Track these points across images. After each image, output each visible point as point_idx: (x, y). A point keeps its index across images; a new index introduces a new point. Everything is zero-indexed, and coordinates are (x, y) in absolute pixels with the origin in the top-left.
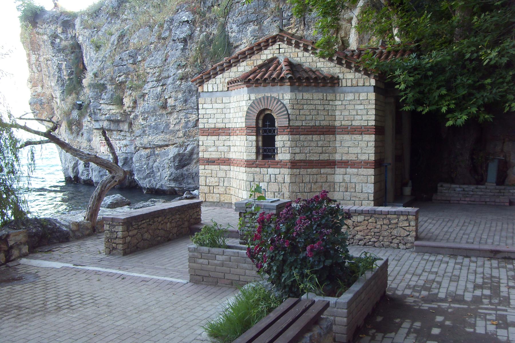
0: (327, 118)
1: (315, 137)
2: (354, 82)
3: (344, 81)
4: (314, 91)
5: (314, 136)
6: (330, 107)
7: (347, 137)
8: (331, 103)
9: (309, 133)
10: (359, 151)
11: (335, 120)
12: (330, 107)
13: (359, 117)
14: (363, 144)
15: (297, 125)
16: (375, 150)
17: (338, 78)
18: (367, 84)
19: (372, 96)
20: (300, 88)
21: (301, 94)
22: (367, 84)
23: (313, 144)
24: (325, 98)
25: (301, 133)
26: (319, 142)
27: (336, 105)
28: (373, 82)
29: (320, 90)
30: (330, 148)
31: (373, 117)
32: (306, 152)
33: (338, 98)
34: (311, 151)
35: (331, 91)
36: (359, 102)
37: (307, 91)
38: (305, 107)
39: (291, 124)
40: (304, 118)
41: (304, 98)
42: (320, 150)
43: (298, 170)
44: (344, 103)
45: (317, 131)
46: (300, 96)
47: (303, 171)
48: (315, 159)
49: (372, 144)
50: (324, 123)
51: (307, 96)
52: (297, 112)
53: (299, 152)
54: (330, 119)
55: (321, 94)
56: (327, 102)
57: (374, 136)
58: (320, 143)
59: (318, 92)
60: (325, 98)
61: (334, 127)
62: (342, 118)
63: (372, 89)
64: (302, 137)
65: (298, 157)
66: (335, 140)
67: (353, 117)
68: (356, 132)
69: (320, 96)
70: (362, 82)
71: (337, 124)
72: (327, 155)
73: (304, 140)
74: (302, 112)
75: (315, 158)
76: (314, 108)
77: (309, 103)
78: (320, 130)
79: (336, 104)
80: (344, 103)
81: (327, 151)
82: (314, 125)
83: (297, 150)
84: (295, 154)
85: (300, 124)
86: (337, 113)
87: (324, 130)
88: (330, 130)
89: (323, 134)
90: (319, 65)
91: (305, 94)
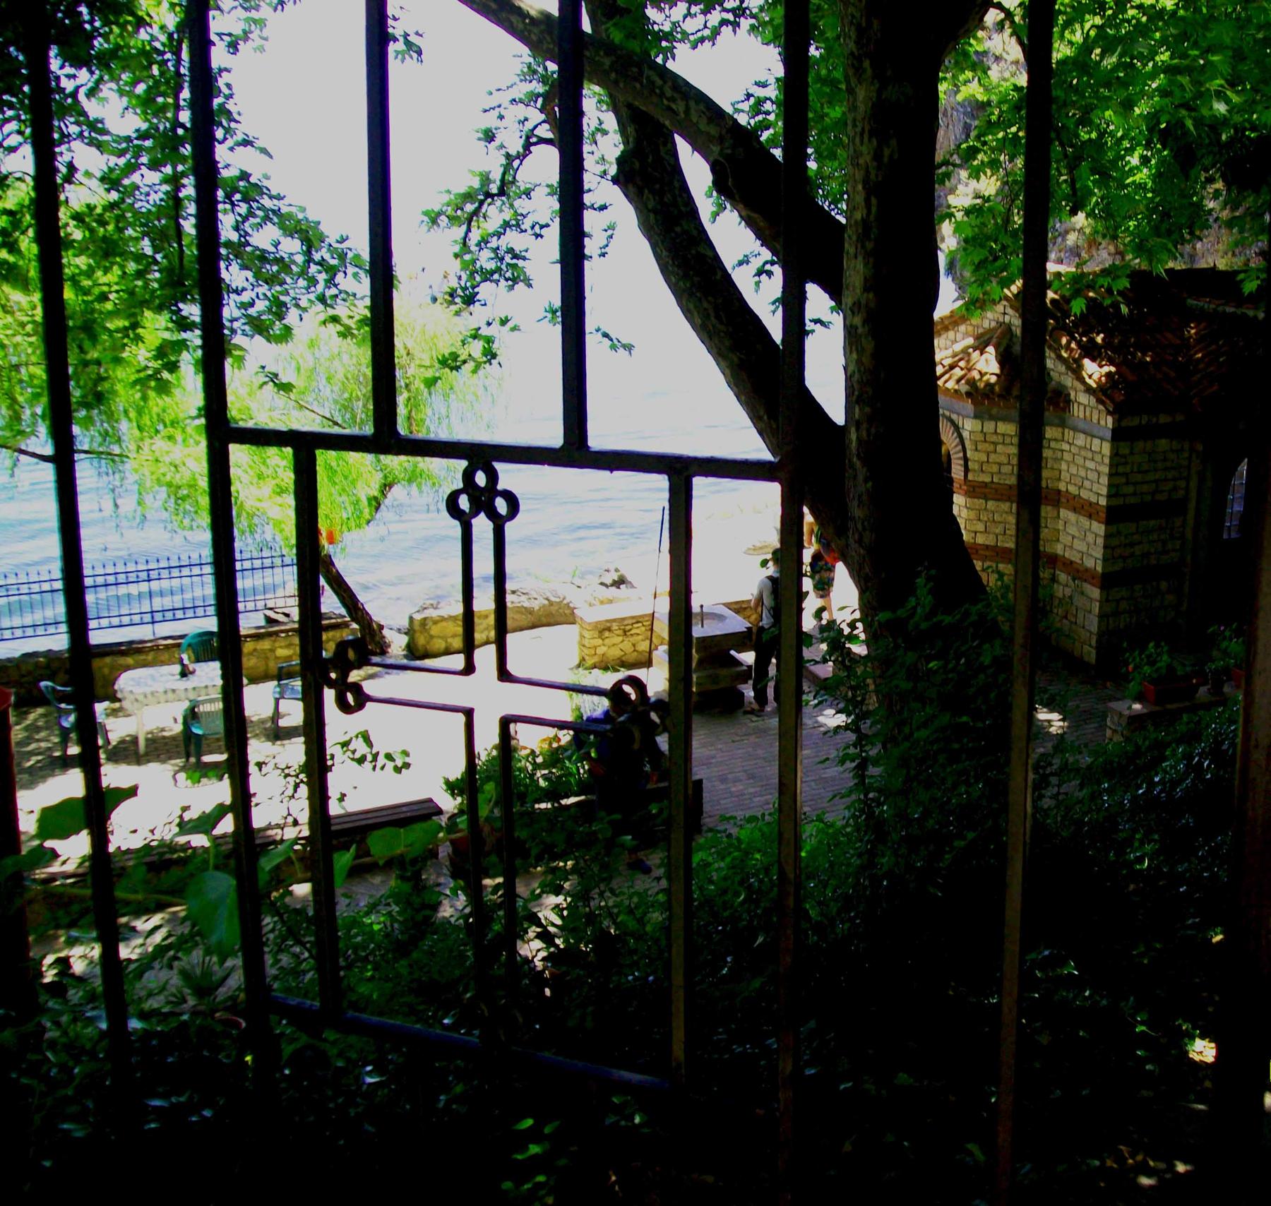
7: (1072, 516)
19: (1106, 448)
21: (993, 423)
22: (1102, 423)
39: (970, 477)
46: (989, 426)
61: (1059, 492)
63: (1109, 435)
71: (1062, 487)
74: (992, 457)
85: (988, 479)
86: (1064, 466)
91: (1000, 424)
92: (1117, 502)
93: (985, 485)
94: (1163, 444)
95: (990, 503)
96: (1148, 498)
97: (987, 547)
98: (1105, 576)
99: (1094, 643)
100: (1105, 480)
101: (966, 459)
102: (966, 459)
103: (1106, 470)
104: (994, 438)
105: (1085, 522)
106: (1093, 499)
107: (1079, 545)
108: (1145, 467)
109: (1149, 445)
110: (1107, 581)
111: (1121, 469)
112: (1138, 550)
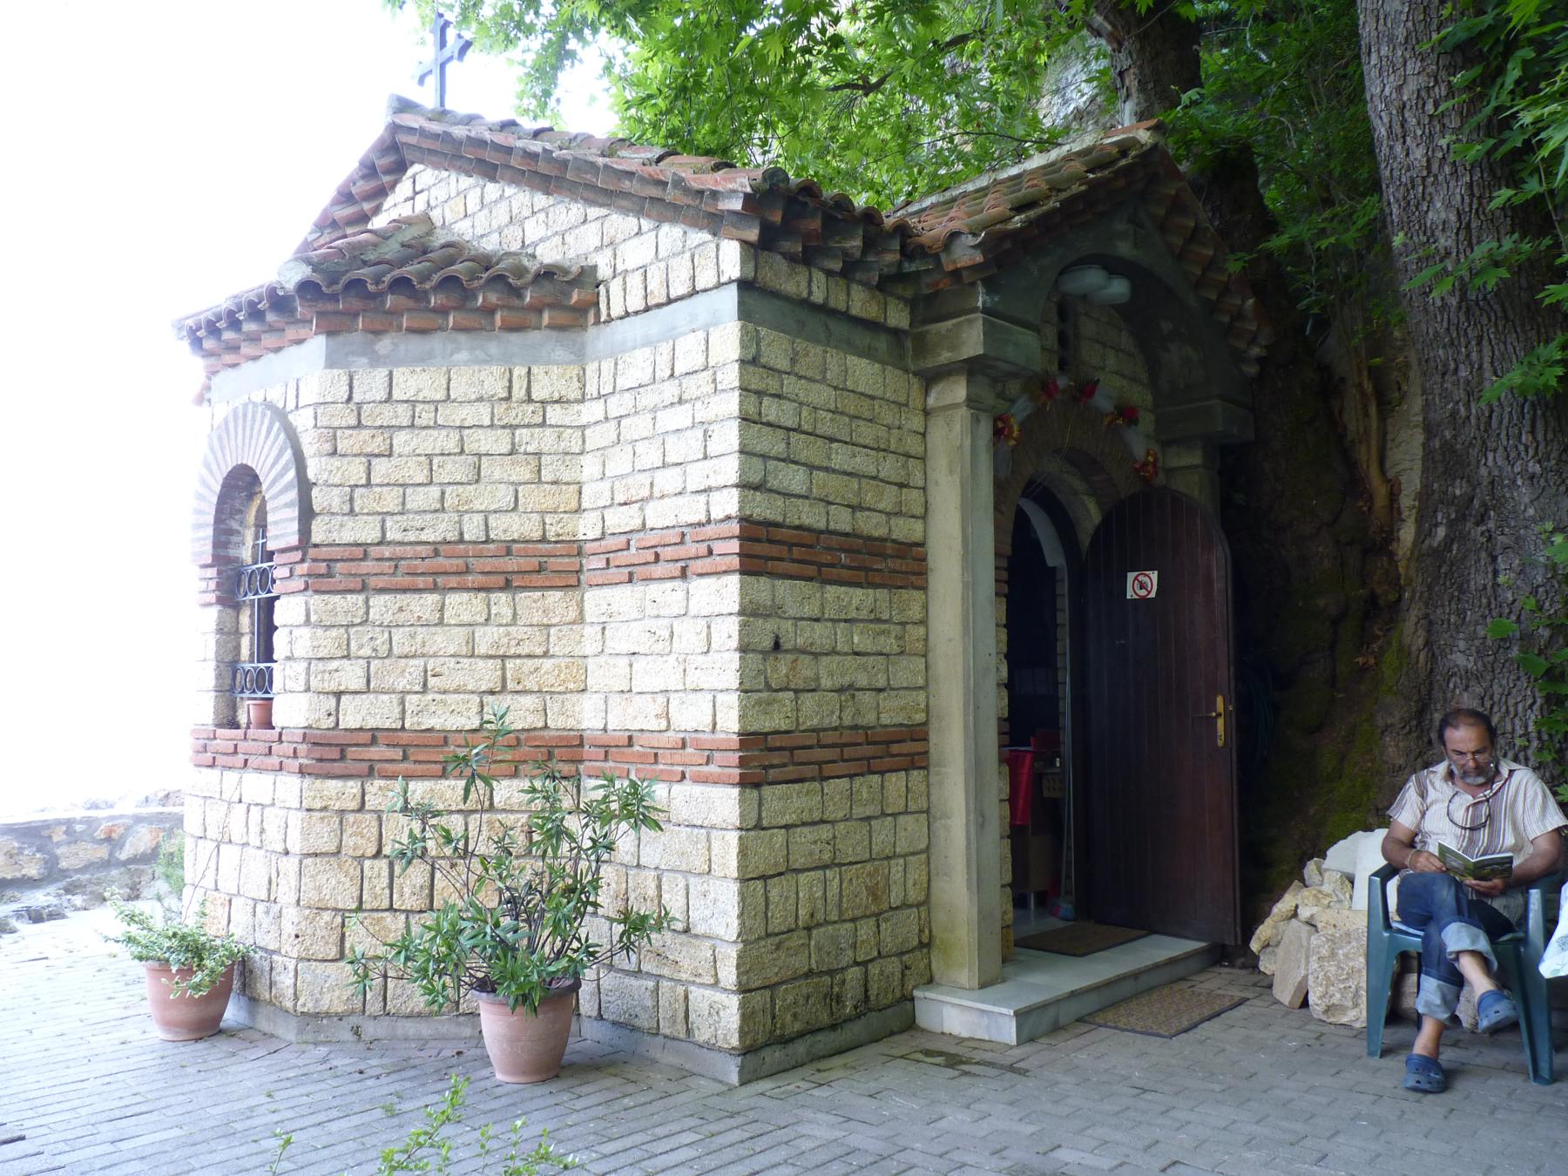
0: (532, 498)
1: (462, 605)
2: (655, 284)
3: (615, 286)
4: (463, 356)
5: (453, 599)
6: (544, 440)
7: (623, 598)
8: (555, 414)
9: (421, 582)
10: (674, 682)
11: (578, 510)
12: (544, 440)
13: (668, 481)
14: (689, 636)
15: (347, 537)
16: (743, 669)
17: (586, 278)
18: (706, 279)
20: (384, 345)
23: (446, 641)
24: (519, 392)
25: (373, 582)
26: (479, 632)
27: (583, 428)
28: (730, 257)
29: (493, 348)
30: (547, 664)
31: (729, 469)
32: (402, 684)
33: (591, 389)
34: (432, 682)
35: (560, 354)
36: (670, 391)
37: (423, 360)
38: (400, 438)
40: (391, 500)
41: (396, 395)
42: (486, 674)
43: (353, 787)
44: (616, 406)
45: (467, 571)
46: (371, 384)
47: (383, 794)
48: (453, 723)
49: (728, 631)
50: (510, 527)
51: (410, 382)
52: (356, 471)
53: (359, 684)
54: (549, 503)
55: (497, 370)
56: (528, 413)
57: (734, 581)
58: (486, 639)
59: (489, 361)
60: (519, 392)
62: (608, 494)
64: (381, 605)
65: (354, 715)
66: (580, 619)
67: (645, 479)
68: (658, 570)
69: (492, 380)
70: (685, 274)
71: (587, 528)
72: (528, 701)
73: (387, 618)
74: (381, 468)
75: (457, 716)
76: (452, 445)
77: (426, 418)
78: (489, 564)
79: (584, 421)
80: (616, 406)
81: (530, 683)
82: (452, 536)
83: (351, 675)
84: (338, 695)
85: (372, 535)
87: (511, 564)
88: (545, 566)
89: (507, 586)
90: (534, 231)
92: (765, 508)
93: (362, 551)
94: (864, 373)
95: (378, 601)
96: (842, 520)
97: (374, 736)
98: (749, 740)
99: (729, 975)
100: (729, 437)
101: (305, 486)
102: (305, 486)
103: (731, 403)
104: (387, 415)
105: (668, 595)
106: (692, 511)
107: (655, 674)
108: (827, 426)
109: (834, 359)
110: (764, 760)
111: (771, 410)
112: (830, 673)
